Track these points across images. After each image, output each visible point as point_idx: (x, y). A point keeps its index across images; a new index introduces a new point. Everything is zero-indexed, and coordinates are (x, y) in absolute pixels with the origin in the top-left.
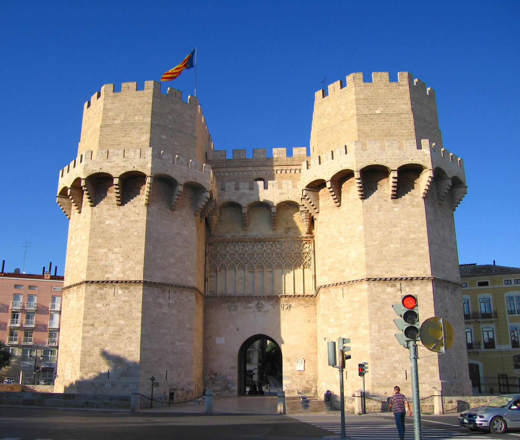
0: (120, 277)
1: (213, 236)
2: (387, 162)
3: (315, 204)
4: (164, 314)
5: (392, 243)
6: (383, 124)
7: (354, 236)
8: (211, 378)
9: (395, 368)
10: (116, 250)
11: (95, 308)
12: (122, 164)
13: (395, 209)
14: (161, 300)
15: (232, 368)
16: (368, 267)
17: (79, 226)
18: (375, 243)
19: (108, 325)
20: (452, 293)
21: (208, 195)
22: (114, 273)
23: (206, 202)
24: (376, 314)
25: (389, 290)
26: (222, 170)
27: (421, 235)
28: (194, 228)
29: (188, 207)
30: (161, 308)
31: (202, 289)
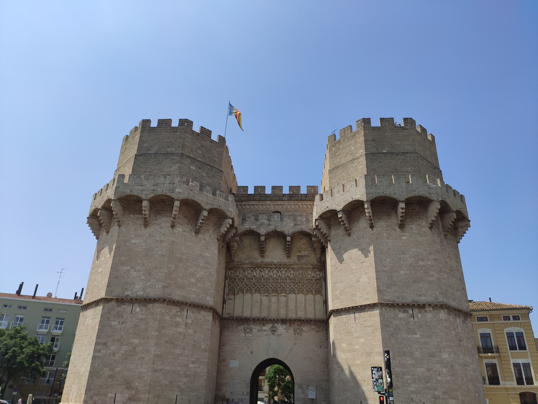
0: (140, 293)
1: (233, 261)
2: (395, 193)
3: (327, 232)
4: (180, 333)
5: (401, 269)
6: (390, 162)
9: (412, 399)
12: (152, 188)
13: (403, 238)
14: (178, 319)
16: (379, 291)
18: (385, 269)
20: (464, 322)
21: (230, 221)
22: (134, 290)
23: (228, 228)
25: (401, 315)
26: (244, 203)
27: (429, 263)
28: (216, 251)
29: (211, 231)
31: (219, 310)
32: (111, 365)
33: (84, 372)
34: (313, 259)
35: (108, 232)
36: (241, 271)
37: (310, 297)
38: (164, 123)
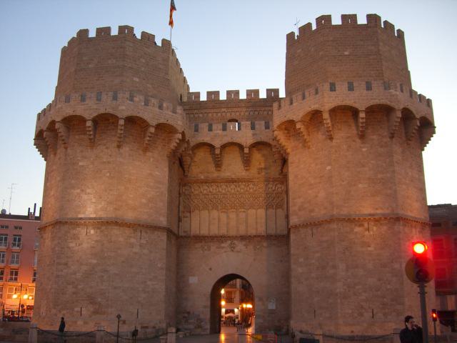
1: (187, 176)
2: (355, 102)
3: (286, 144)
4: (136, 253)
5: (360, 183)
7: (323, 176)
8: (184, 317)
10: (88, 191)
11: (69, 248)
13: (364, 149)
14: (133, 240)
15: (205, 307)
17: (54, 167)
19: (81, 264)
21: (180, 136)
22: (87, 213)
23: (177, 143)
24: (344, 253)
27: (388, 175)
28: (167, 169)
30: (133, 247)
31: (175, 230)
32: (73, 283)
33: (51, 289)
34: (275, 171)
35: (55, 154)
36: (197, 188)
37: (271, 211)
38: (104, 32)
